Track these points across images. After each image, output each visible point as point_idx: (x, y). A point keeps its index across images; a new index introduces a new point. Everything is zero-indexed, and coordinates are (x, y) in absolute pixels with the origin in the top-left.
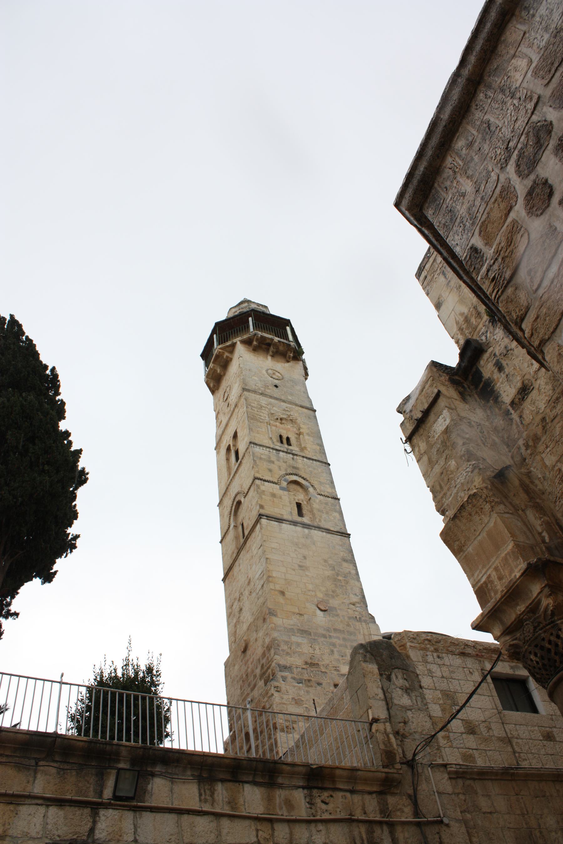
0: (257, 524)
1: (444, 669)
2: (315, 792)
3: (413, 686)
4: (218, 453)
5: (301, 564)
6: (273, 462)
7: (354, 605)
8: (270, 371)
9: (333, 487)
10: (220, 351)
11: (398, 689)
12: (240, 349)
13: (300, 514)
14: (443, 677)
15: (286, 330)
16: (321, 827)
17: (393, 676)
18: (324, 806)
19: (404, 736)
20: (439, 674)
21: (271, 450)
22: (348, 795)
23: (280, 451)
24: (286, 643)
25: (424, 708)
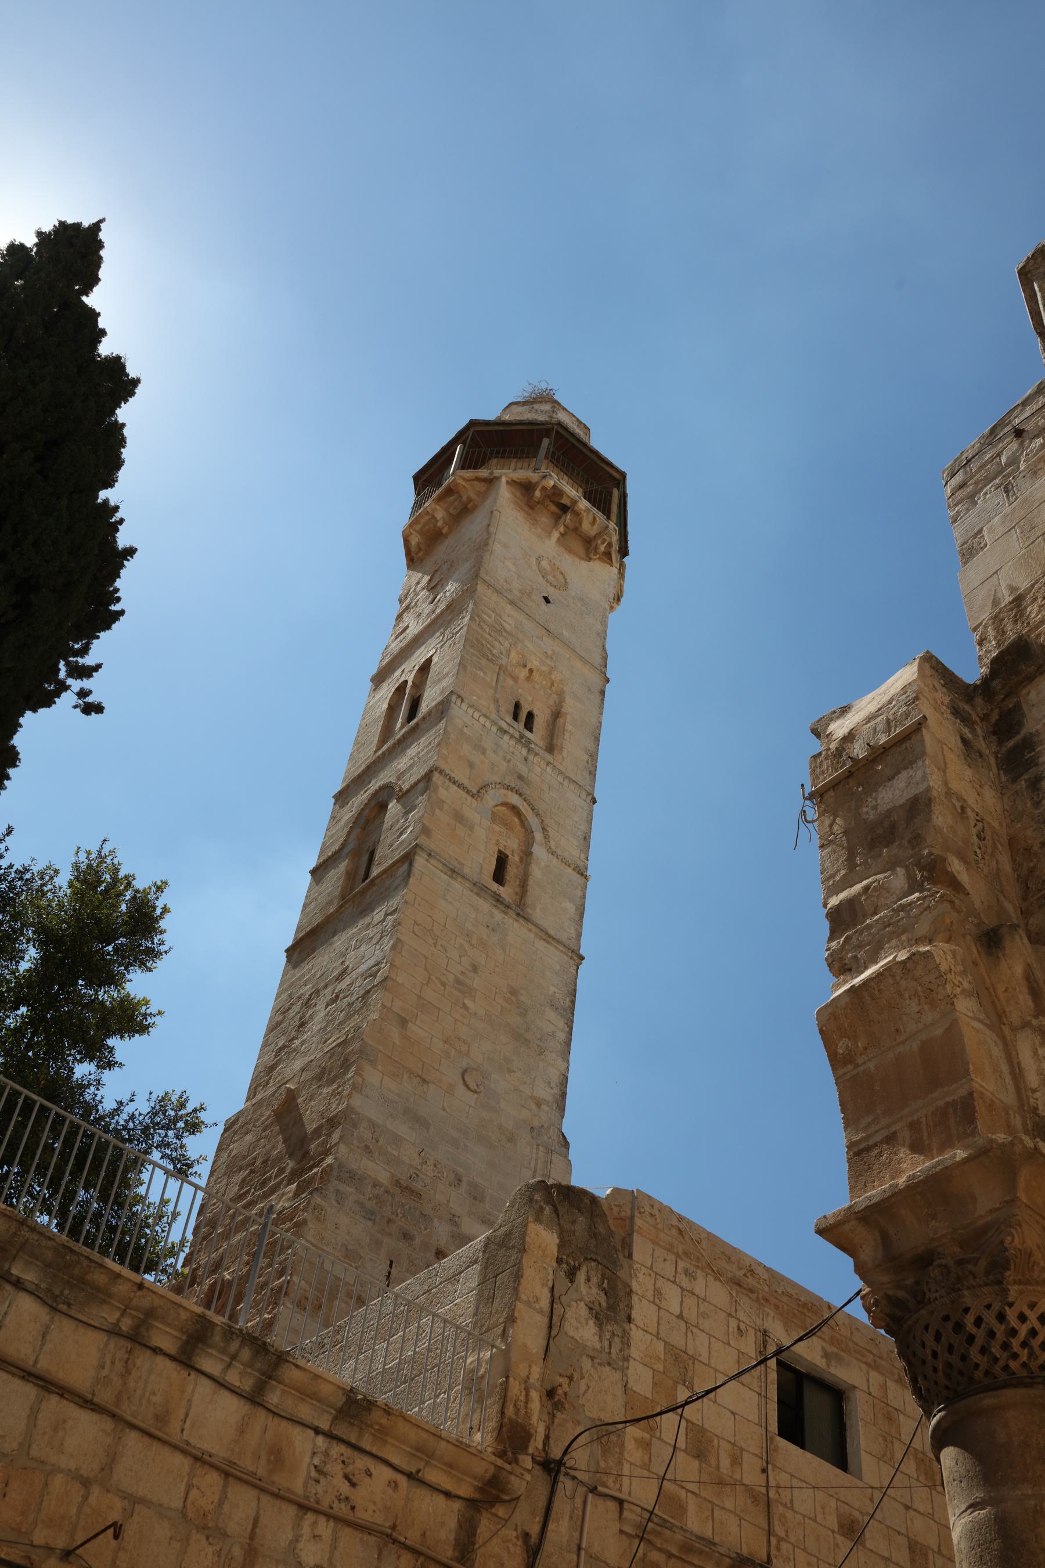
0: (403, 863)
1: (690, 1302)
2: (337, 1450)
3: (614, 1309)
5: (461, 977)
6: (484, 752)
7: (538, 1105)
8: (545, 564)
10: (460, 481)
11: (582, 1304)
12: (504, 493)
13: (499, 876)
14: (680, 1317)
15: (611, 494)
16: (325, 1528)
17: (581, 1276)
18: (345, 1487)
19: (558, 1406)
20: (674, 1305)
21: (488, 724)
22: (402, 1480)
23: (505, 732)
24: (373, 1125)
25: (620, 1362)
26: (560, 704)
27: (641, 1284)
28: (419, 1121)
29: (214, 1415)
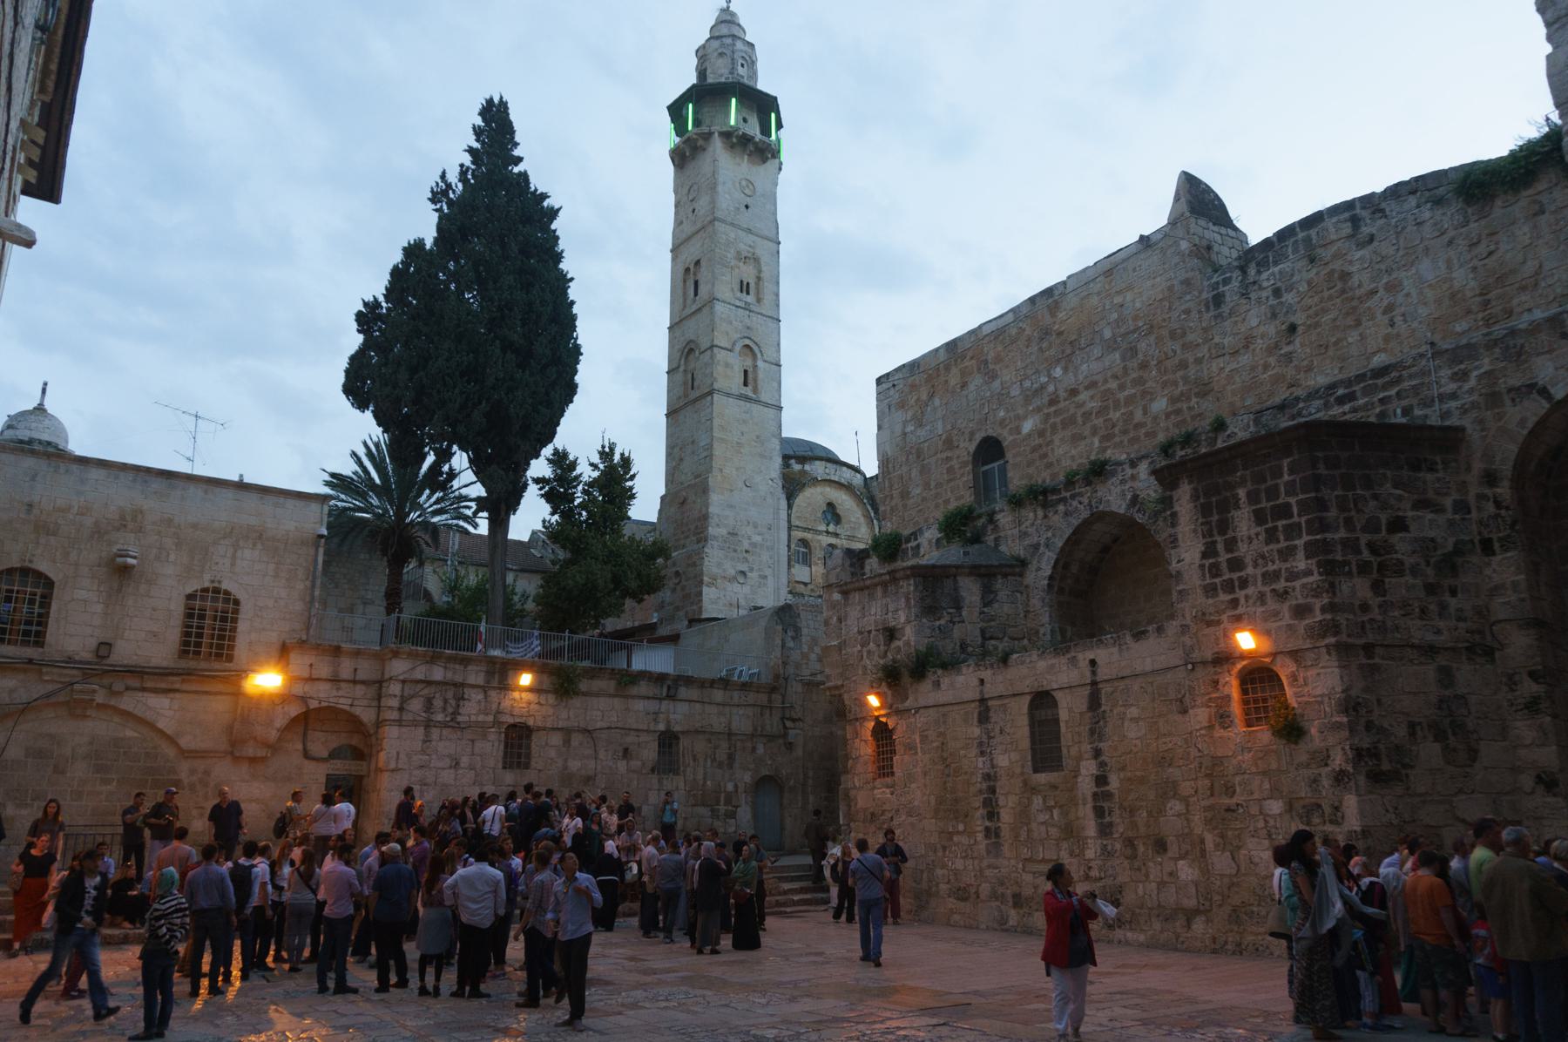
3: (797, 636)
4: (674, 259)
9: (778, 351)
12: (717, 144)
13: (746, 384)
26: (760, 271)
27: (803, 624)
28: (731, 506)
29: (718, 695)
